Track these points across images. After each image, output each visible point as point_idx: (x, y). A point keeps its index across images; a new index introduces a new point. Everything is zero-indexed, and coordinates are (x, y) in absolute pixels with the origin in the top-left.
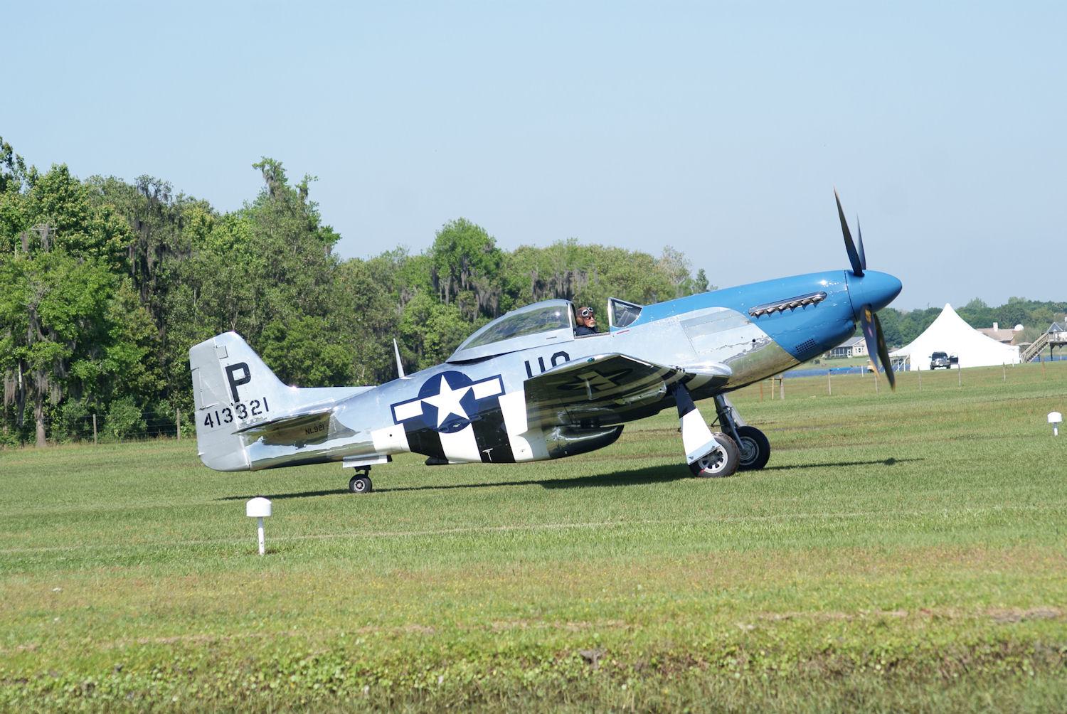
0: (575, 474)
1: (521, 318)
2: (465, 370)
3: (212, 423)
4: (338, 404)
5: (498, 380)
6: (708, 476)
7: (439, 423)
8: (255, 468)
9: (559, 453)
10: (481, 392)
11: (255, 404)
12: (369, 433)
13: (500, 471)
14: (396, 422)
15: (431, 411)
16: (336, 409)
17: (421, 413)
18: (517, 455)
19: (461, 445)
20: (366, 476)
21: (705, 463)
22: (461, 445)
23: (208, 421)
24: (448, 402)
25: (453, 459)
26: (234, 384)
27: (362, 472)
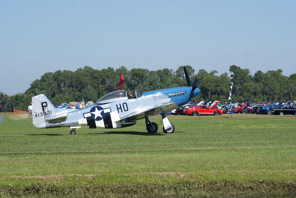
2: (102, 106)
3: (37, 116)
5: (109, 109)
7: (95, 119)
8: (47, 128)
9: (123, 126)
10: (106, 111)
12: (77, 120)
14: (85, 118)
15: (93, 115)
17: (90, 115)
19: (100, 124)
22: (100, 124)
23: (36, 116)
24: (97, 113)
25: (98, 127)
27: (73, 129)
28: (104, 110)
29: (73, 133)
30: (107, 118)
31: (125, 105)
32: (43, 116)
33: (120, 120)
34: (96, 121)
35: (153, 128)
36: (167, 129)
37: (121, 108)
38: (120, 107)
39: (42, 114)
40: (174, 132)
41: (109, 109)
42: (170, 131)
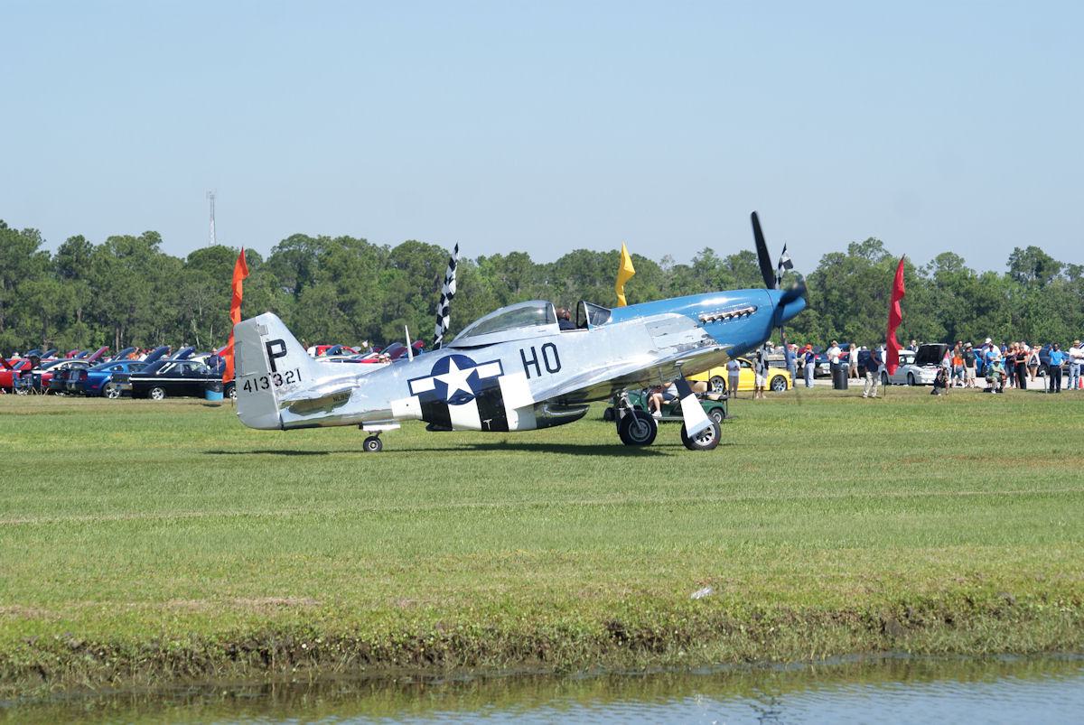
0: (546, 441)
2: (470, 354)
3: (250, 388)
5: (497, 364)
6: (704, 448)
7: (449, 397)
9: (543, 424)
10: (485, 372)
11: (290, 375)
12: (388, 402)
13: (497, 437)
14: (412, 395)
15: (442, 387)
17: (432, 387)
19: (466, 415)
21: (698, 438)
24: (456, 380)
26: (272, 356)
27: (374, 435)
28: (479, 369)
29: (373, 446)
30: (489, 398)
31: (549, 350)
33: (533, 402)
34: (451, 407)
35: (639, 431)
37: (535, 361)
39: (280, 379)
41: (497, 364)
42: (707, 439)
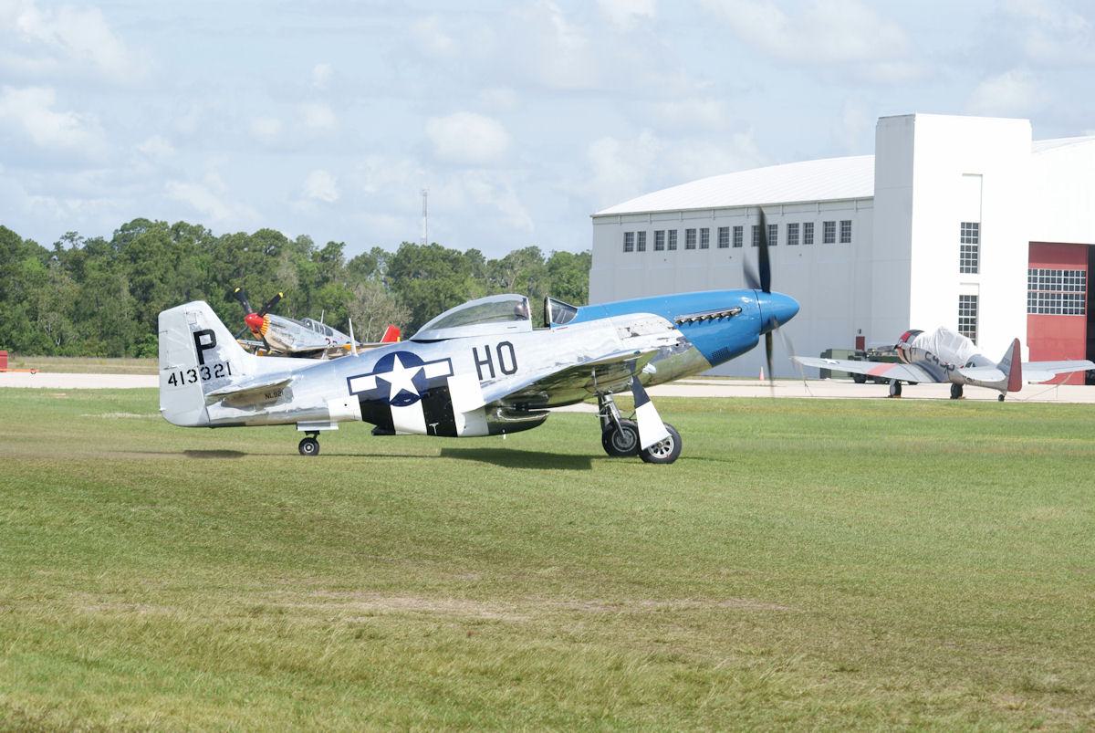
1: (471, 309)
3: (176, 382)
4: (294, 373)
7: (391, 399)
9: (496, 430)
10: (432, 372)
11: (219, 368)
14: (351, 394)
16: (294, 377)
18: (460, 429)
19: (410, 418)
20: (313, 441)
23: (172, 380)
27: (312, 436)
28: (425, 367)
29: (309, 448)
30: (436, 400)
31: (505, 350)
32: (200, 383)
33: (484, 404)
35: (623, 441)
36: (653, 447)
37: (489, 361)
38: (486, 359)
40: (681, 455)
42: (662, 453)
